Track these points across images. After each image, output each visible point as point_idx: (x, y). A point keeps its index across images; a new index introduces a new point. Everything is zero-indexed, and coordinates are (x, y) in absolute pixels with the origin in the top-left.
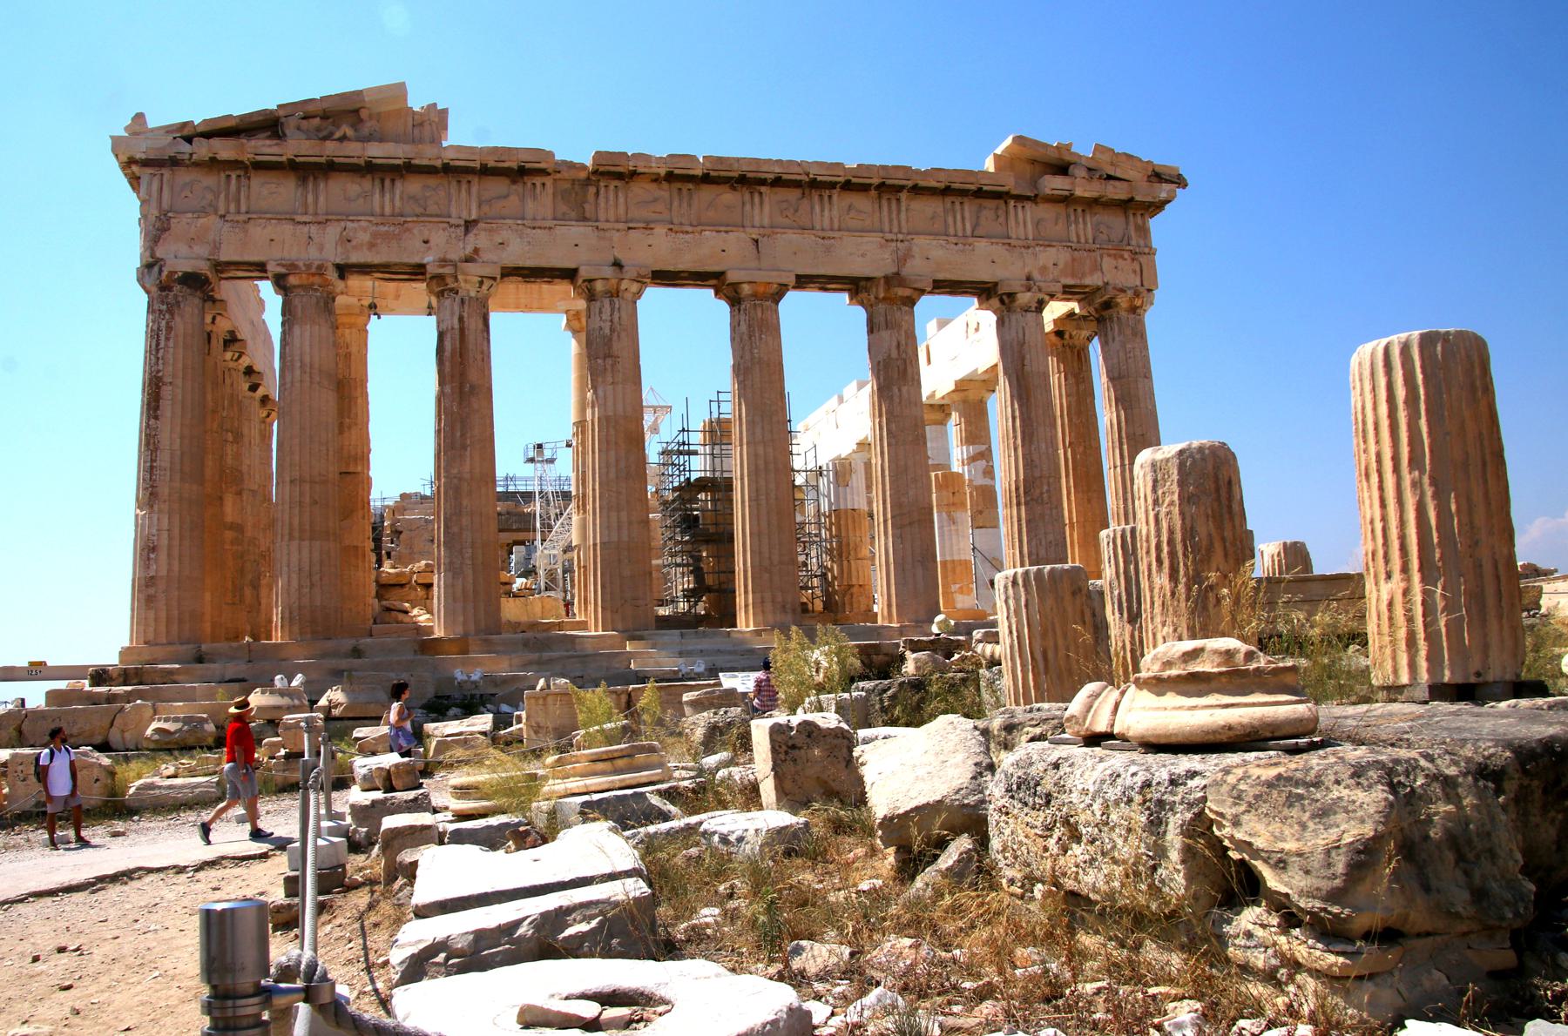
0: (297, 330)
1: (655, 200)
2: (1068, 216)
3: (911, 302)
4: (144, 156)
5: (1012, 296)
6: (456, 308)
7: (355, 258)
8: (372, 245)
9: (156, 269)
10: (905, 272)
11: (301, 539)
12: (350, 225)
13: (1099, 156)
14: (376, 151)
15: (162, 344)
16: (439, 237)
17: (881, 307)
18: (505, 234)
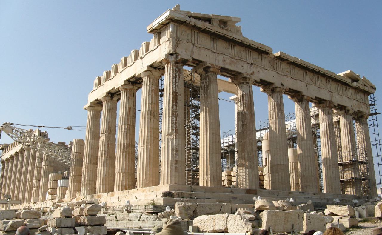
0: (211, 85)
1: (288, 69)
2: (356, 93)
3: (332, 107)
4: (178, 19)
5: (349, 110)
6: (248, 88)
7: (228, 67)
8: (230, 64)
9: (175, 56)
10: (333, 100)
11: (216, 154)
12: (225, 56)
13: (364, 79)
14: (235, 36)
15: (177, 81)
16: (246, 66)
17: (327, 109)
18: (259, 69)
